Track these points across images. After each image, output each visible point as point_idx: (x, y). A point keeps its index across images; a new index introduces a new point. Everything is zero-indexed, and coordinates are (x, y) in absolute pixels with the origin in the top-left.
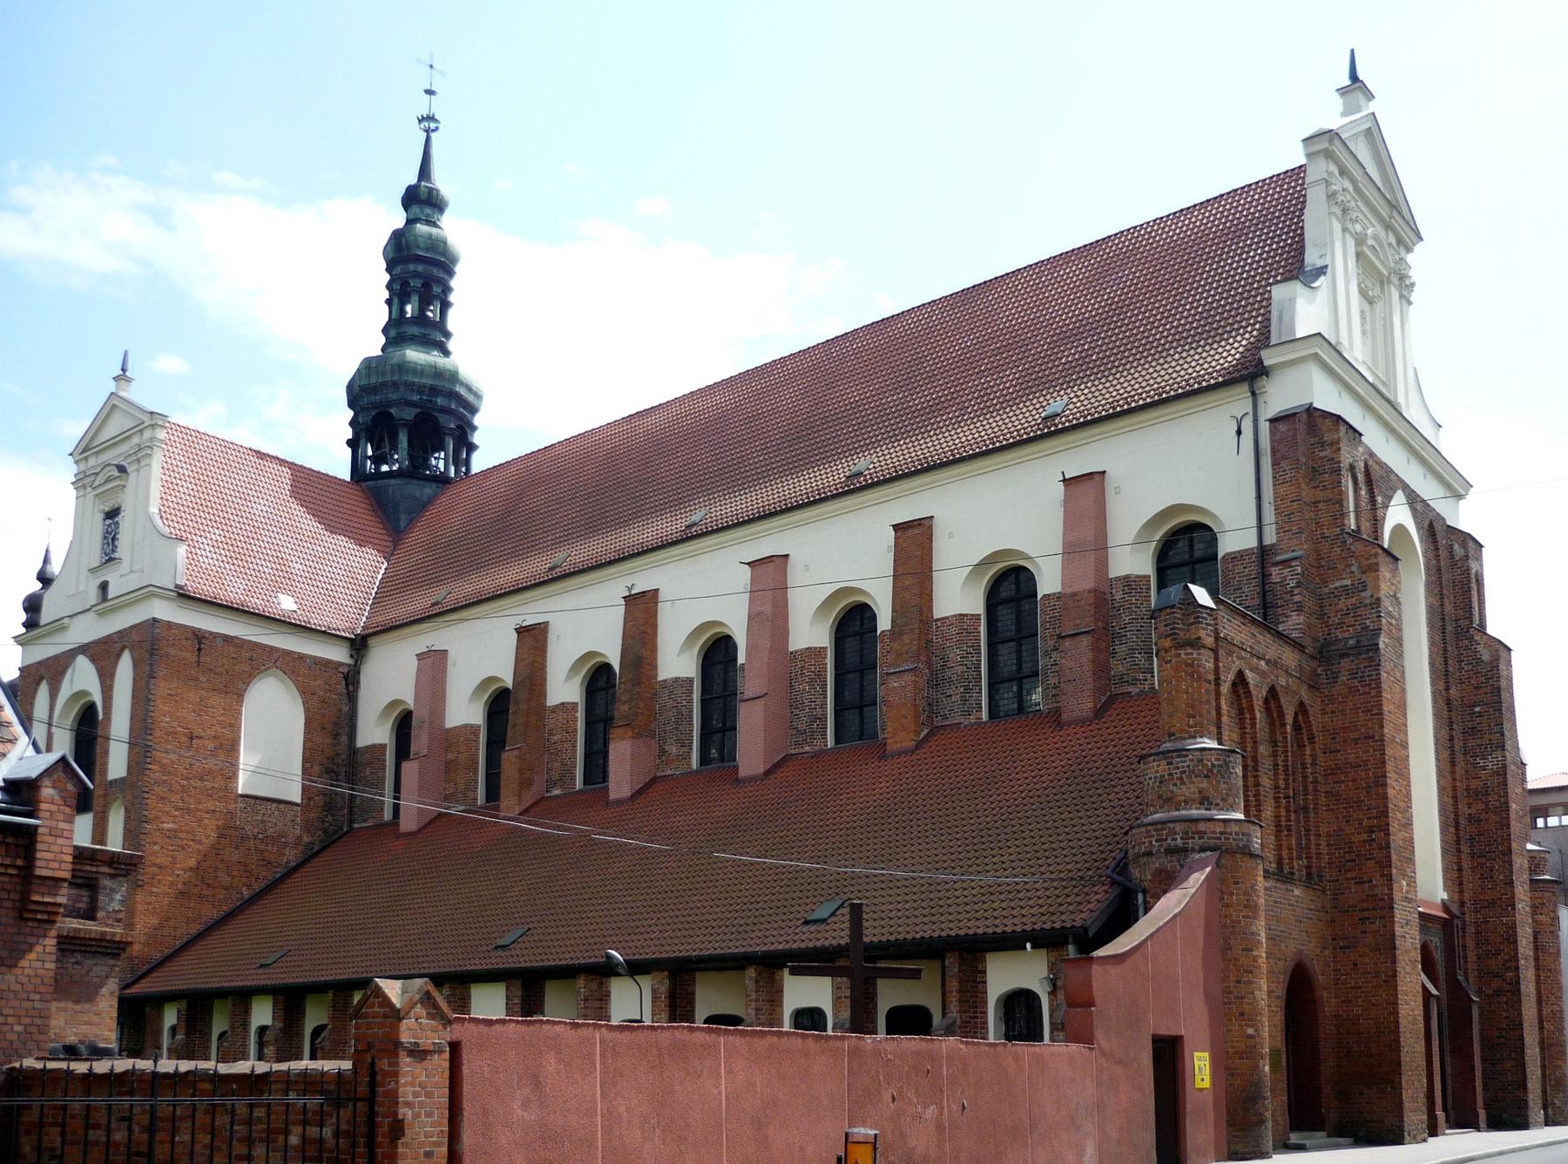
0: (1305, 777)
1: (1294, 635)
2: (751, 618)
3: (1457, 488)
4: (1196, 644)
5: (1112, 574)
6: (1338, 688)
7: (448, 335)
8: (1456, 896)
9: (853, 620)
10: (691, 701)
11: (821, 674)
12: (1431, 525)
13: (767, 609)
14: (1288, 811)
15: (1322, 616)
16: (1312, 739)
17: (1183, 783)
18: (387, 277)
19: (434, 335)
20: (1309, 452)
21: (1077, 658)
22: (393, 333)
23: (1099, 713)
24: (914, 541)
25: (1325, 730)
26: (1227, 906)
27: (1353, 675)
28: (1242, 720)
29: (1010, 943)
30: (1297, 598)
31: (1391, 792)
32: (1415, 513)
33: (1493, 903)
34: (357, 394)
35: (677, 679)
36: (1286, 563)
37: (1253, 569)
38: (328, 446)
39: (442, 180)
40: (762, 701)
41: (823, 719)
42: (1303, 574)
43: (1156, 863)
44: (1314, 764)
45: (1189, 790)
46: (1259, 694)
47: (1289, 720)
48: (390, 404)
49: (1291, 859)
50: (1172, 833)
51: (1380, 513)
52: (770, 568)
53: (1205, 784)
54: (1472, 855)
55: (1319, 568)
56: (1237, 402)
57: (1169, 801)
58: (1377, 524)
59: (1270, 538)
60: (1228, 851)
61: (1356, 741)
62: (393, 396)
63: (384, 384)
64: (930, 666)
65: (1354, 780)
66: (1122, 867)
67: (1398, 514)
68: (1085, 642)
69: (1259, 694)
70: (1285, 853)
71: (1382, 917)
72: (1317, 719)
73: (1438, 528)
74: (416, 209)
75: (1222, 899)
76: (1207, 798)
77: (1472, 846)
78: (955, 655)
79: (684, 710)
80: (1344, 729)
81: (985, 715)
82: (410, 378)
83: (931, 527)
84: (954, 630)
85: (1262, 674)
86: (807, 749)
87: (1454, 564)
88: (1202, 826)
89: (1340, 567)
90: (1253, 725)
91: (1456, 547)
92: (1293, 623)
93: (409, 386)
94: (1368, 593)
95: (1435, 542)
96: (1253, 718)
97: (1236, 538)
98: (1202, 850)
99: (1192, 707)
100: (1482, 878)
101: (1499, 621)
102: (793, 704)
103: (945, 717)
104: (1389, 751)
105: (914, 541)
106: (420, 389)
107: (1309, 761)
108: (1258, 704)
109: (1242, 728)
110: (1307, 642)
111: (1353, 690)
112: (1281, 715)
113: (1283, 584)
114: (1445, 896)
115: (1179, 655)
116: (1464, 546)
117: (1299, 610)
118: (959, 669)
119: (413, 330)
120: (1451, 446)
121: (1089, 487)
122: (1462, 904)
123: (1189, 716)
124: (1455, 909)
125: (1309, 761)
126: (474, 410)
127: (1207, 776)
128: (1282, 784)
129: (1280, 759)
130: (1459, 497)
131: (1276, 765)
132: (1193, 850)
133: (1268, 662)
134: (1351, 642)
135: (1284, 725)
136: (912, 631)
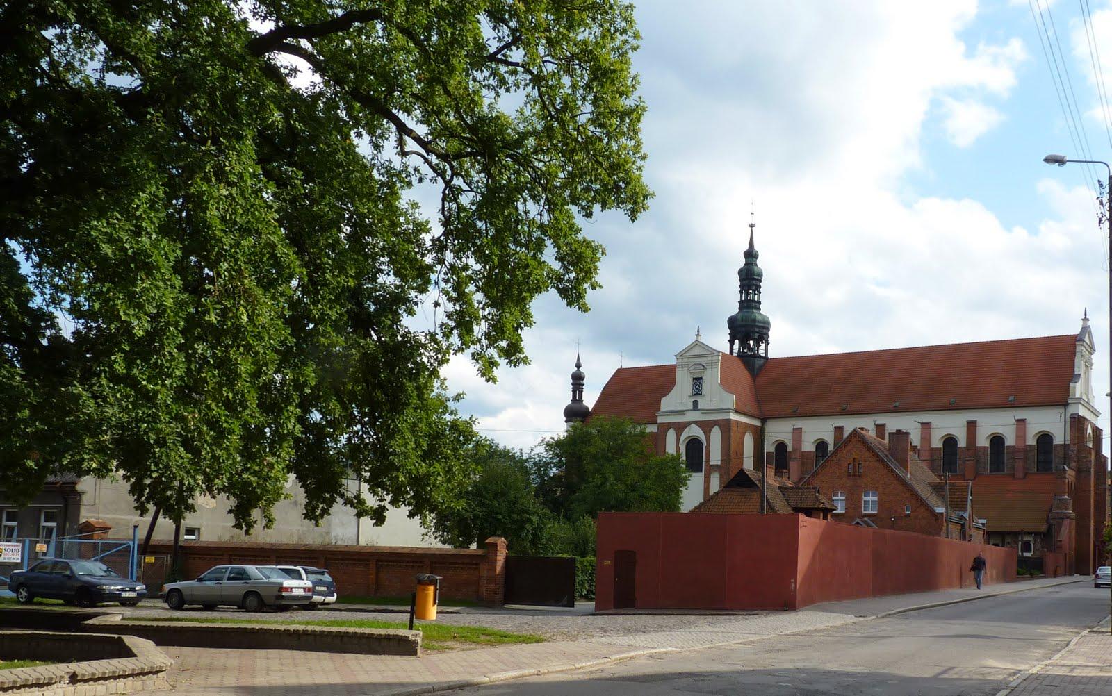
2: (922, 438)
5: (1027, 444)
7: (760, 303)
18: (739, 283)
19: (756, 305)
20: (1078, 423)
21: (1019, 465)
23: (1024, 477)
24: (972, 426)
29: (1029, 533)
34: (732, 322)
36: (1073, 451)
37: (1062, 448)
38: (720, 340)
39: (757, 247)
55: (1079, 452)
59: (1068, 442)
67: (1089, 431)
97: (1059, 439)
105: (972, 426)
121: (1022, 423)
126: (768, 329)
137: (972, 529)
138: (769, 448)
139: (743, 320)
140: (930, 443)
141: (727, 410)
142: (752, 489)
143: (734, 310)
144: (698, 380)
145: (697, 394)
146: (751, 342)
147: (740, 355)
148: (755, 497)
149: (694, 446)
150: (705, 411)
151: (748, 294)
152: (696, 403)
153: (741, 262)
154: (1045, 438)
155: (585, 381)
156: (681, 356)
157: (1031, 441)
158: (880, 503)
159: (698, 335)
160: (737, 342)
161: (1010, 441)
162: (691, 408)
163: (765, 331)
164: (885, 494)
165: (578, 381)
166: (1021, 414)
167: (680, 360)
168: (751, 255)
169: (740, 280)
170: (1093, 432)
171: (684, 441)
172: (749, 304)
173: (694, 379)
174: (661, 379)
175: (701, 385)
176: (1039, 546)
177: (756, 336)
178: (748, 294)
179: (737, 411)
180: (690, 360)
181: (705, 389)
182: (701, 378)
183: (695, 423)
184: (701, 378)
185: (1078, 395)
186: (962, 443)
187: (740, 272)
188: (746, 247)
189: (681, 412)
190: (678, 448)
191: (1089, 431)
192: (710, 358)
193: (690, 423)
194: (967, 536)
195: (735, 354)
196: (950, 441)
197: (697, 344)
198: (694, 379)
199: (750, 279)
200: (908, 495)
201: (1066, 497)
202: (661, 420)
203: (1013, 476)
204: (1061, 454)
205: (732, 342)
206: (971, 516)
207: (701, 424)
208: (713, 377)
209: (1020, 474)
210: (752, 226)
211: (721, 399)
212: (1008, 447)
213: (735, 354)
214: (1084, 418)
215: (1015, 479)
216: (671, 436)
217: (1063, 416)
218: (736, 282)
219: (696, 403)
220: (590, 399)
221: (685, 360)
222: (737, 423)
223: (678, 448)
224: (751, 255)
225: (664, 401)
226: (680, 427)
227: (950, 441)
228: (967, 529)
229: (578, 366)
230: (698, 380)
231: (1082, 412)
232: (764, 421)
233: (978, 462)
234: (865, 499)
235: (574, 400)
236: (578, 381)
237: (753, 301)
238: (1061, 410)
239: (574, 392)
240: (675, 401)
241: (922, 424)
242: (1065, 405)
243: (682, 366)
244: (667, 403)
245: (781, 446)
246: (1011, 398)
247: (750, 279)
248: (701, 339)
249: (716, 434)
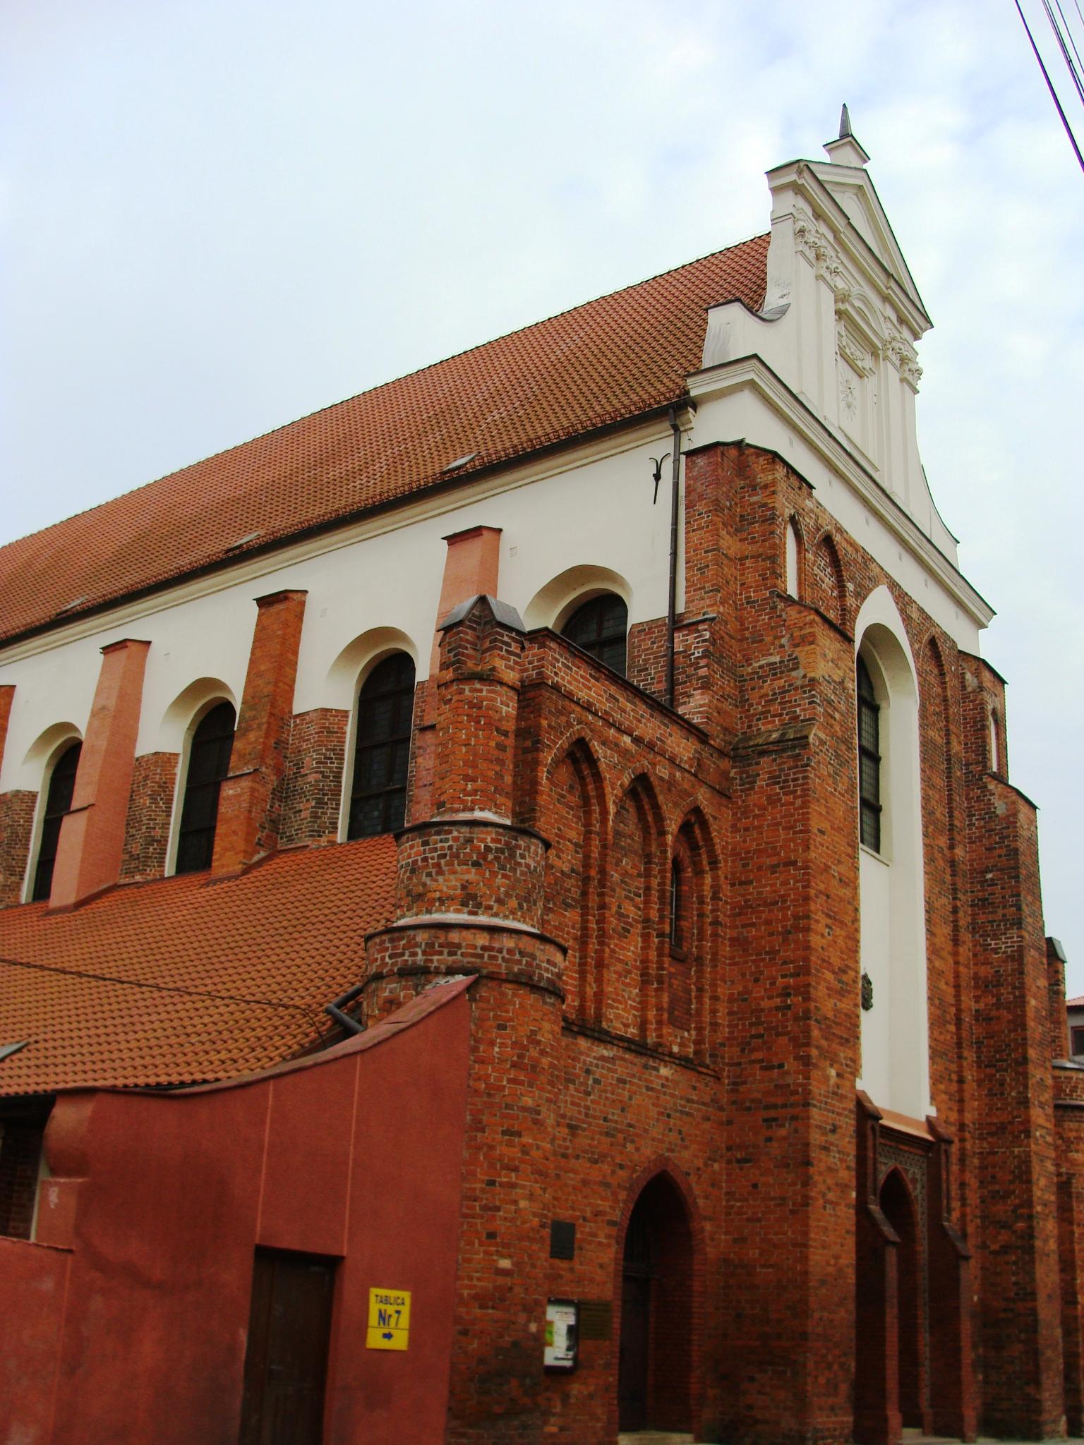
0: (701, 915)
1: (696, 720)
3: (977, 612)
4: (490, 678)
6: (753, 797)
8: (954, 1116)
9: (213, 722)
10: (30, 820)
11: (166, 788)
12: (933, 642)
13: (112, 703)
14: (660, 955)
15: (742, 702)
16: (714, 863)
17: (440, 872)
25: (735, 854)
26: (482, 1062)
27: (774, 780)
28: (588, 813)
30: (703, 672)
31: (815, 940)
32: (907, 619)
33: (1002, 1128)
35: (17, 793)
40: (85, 814)
41: (163, 842)
42: (713, 641)
43: (388, 989)
44: (715, 897)
45: (448, 883)
46: (616, 783)
47: (672, 826)
49: (660, 1023)
50: (412, 944)
51: (850, 601)
52: (121, 655)
53: (472, 875)
54: (979, 1062)
57: (419, 899)
58: (848, 615)
60: (492, 977)
61: (773, 869)
64: (279, 771)
65: (768, 922)
67: (877, 609)
69: (616, 783)
70: (651, 1014)
71: (794, 1118)
72: (722, 834)
73: (944, 649)
75: (475, 1049)
76: (473, 897)
77: (979, 1051)
78: (310, 761)
79: (20, 830)
80: (758, 851)
81: (341, 836)
83: (303, 604)
84: (313, 729)
85: (624, 753)
86: (138, 878)
87: (965, 697)
88: (455, 936)
89: (768, 639)
90: (604, 821)
91: (968, 676)
92: (695, 705)
94: (801, 672)
95: (940, 666)
96: (604, 812)
97: (646, 604)
98: (451, 971)
99: (474, 767)
100: (990, 1094)
102: (132, 822)
103: (290, 839)
104: (818, 884)
107: (707, 892)
108: (612, 795)
109: (587, 824)
110: (713, 729)
111: (773, 800)
112: (659, 819)
113: (686, 654)
114: (933, 1112)
115: (461, 692)
116: (977, 674)
117: (706, 686)
118: (311, 778)
120: (969, 560)
122: (962, 1127)
123: (467, 778)
124: (949, 1131)
125: (707, 892)
127: (476, 864)
128: (654, 915)
129: (655, 882)
130: (981, 626)
131: (648, 888)
132: (437, 972)
133: (637, 740)
134: (775, 736)
135: (662, 833)
136: (259, 726)
140: (130, 737)
231: (764, 432)
233: (284, 791)
242: (676, 409)
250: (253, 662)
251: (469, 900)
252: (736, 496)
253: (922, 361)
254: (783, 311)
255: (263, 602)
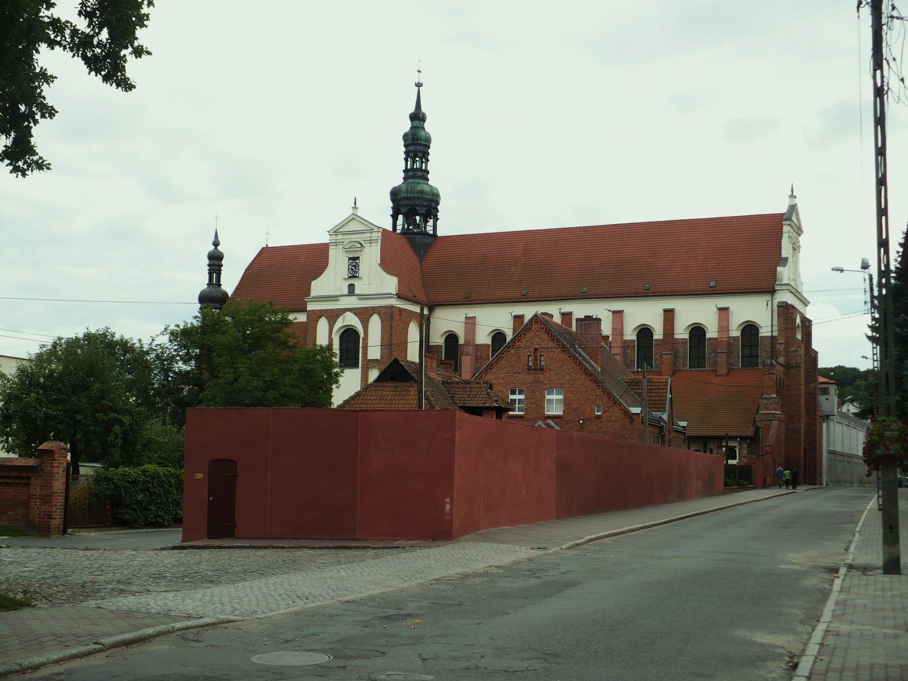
3: (805, 303)
7: (428, 172)
18: (404, 149)
19: (424, 174)
21: (722, 359)
22: (411, 173)
24: (669, 315)
29: (734, 438)
34: (395, 194)
36: (781, 344)
38: (380, 214)
39: (424, 109)
45: (771, 407)
48: (417, 205)
55: (787, 344)
56: (768, 297)
57: (767, 409)
59: (775, 334)
62: (417, 202)
63: (414, 198)
66: (754, 421)
67: (798, 321)
68: (724, 355)
74: (417, 123)
78: (681, 350)
82: (425, 196)
92: (781, 360)
93: (424, 199)
97: (765, 331)
101: (815, 346)
102: (625, 356)
105: (669, 315)
106: (426, 200)
119: (419, 174)
137: (673, 434)
138: (437, 339)
139: (407, 191)
140: (622, 335)
141: (387, 296)
142: (408, 384)
143: (398, 179)
144: (354, 261)
145: (353, 277)
146: (418, 218)
147: (404, 232)
148: (412, 393)
149: (350, 337)
150: (362, 297)
151: (414, 162)
152: (351, 287)
153: (407, 126)
154: (750, 329)
155: (223, 262)
156: (335, 232)
157: (735, 333)
158: (567, 403)
159: (355, 208)
160: (400, 217)
161: (712, 333)
162: (346, 292)
163: (433, 204)
164: (572, 392)
165: (215, 261)
166: (723, 302)
167: (334, 237)
168: (417, 117)
169: (405, 146)
170: (802, 321)
171: (337, 332)
172: (416, 173)
173: (350, 259)
174: (313, 259)
175: (356, 266)
176: (745, 452)
177: (423, 211)
178: (414, 162)
179: (399, 296)
180: (345, 237)
181: (363, 271)
182: (358, 258)
183: (350, 310)
184: (358, 258)
185: (785, 281)
186: (658, 335)
187: (405, 136)
188: (412, 109)
189: (335, 298)
190: (331, 340)
191: (798, 321)
192: (368, 235)
193: (344, 311)
194: (667, 441)
195: (398, 231)
196: (645, 332)
197: (354, 218)
198: (350, 259)
199: (417, 145)
200: (599, 392)
201: (774, 395)
202: (310, 307)
203: (715, 372)
204: (768, 347)
205: (395, 217)
206: (671, 417)
207: (357, 312)
208: (371, 257)
209: (723, 370)
210: (419, 85)
211: (379, 284)
212: (710, 339)
213: (398, 231)
214: (793, 307)
215: (716, 375)
216: (323, 325)
217: (770, 303)
218: (400, 149)
219: (351, 287)
220: (230, 282)
221: (340, 237)
222: (400, 310)
223: (331, 340)
224: (417, 117)
225: (314, 284)
226: (333, 316)
227: (645, 332)
228: (666, 432)
229: (216, 244)
230: (354, 261)
232: (431, 310)
233: (675, 356)
234: (548, 397)
235: (210, 283)
236: (215, 261)
237: (420, 170)
238: (768, 298)
239: (210, 274)
240: (328, 284)
241: (614, 312)
242: (772, 292)
243: (336, 244)
244: (318, 287)
245: (451, 338)
246: (712, 284)
247: (417, 145)
248: (359, 213)
249: (375, 323)
250: (664, 326)
251: (775, 410)
252: (786, 312)
253: (801, 244)
254: (786, 259)
255: (666, 311)
